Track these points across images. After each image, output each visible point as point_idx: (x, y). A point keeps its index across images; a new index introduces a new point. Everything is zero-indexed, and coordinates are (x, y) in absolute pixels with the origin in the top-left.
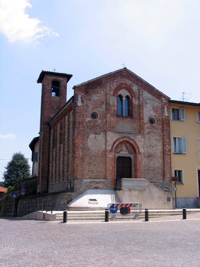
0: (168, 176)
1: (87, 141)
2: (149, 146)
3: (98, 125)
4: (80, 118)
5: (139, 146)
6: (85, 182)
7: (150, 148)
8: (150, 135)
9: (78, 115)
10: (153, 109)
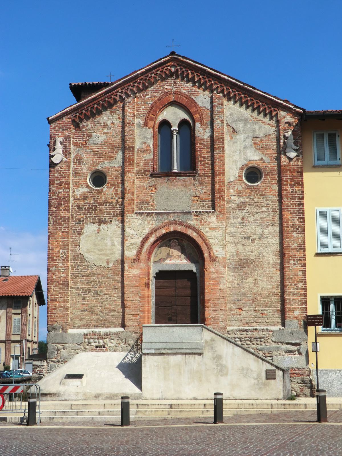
0: (297, 313)
1: (80, 241)
2: (240, 240)
3: (106, 202)
4: (61, 190)
5: (211, 241)
6: (73, 336)
7: (243, 245)
8: (245, 211)
9: (57, 184)
10: (255, 144)
